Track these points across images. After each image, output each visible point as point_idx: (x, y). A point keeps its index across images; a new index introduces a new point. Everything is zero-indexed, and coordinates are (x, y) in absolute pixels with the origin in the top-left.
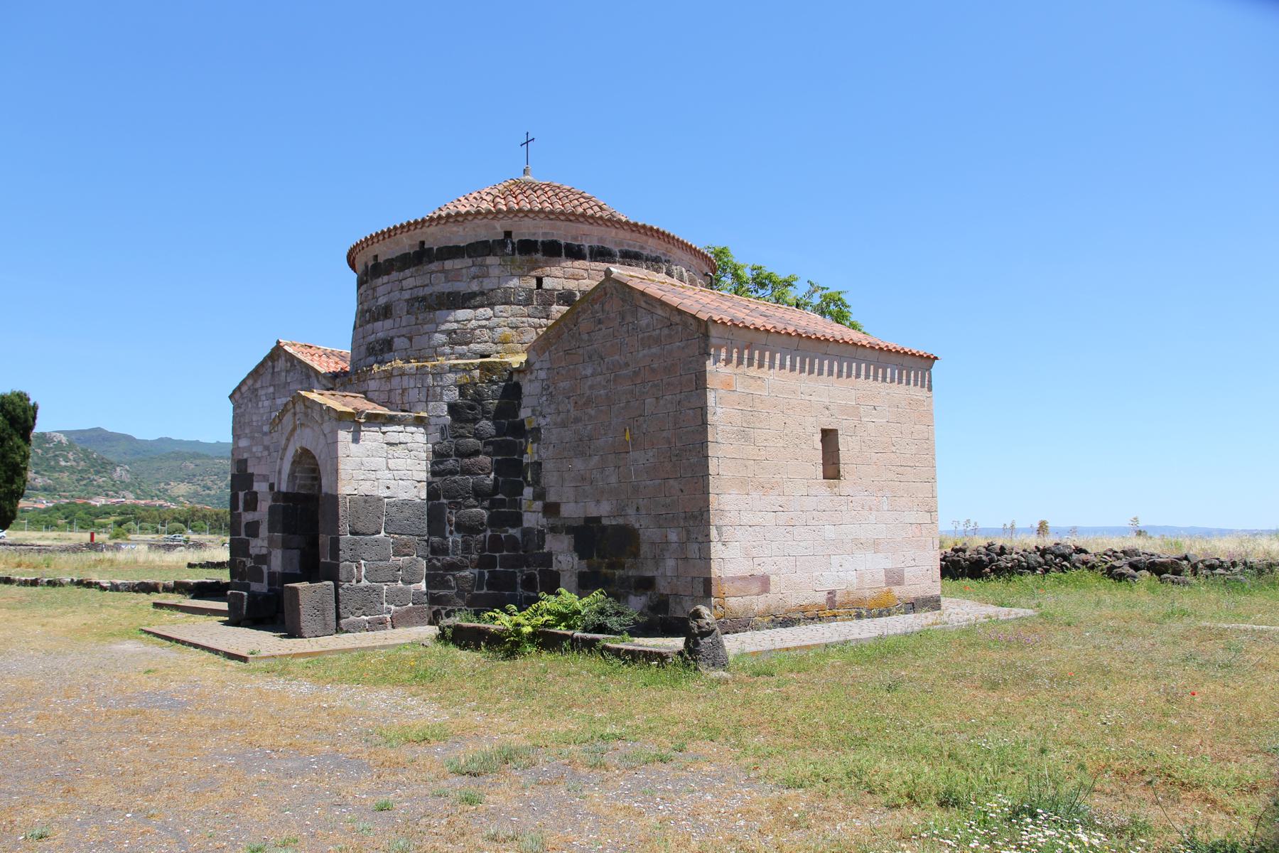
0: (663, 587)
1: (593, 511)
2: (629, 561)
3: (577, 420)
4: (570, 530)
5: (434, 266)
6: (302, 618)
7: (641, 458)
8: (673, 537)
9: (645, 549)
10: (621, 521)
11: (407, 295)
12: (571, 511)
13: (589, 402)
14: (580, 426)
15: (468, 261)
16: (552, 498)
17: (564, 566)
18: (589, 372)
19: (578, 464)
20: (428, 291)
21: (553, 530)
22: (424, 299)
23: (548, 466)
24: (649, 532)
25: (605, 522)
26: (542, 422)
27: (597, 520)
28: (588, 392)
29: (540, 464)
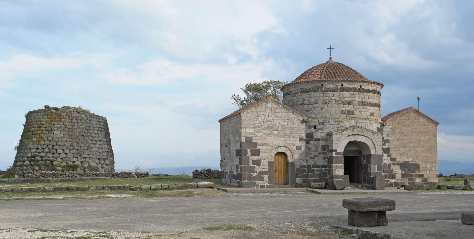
0: (425, 176)
1: (406, 160)
2: (416, 171)
3: (401, 139)
4: (398, 164)
5: (365, 93)
6: (377, 184)
7: (420, 150)
8: (429, 166)
9: (421, 169)
10: (415, 163)
11: (357, 100)
12: (400, 160)
13: (405, 135)
14: (402, 141)
15: (371, 94)
16: (393, 156)
17: (397, 172)
18: (406, 129)
19: (402, 150)
20: (364, 100)
21: (394, 164)
22: (363, 102)
23: (391, 150)
24: (422, 166)
25: (410, 163)
26: (390, 138)
27: (408, 162)
28: (405, 133)
29: (389, 148)
